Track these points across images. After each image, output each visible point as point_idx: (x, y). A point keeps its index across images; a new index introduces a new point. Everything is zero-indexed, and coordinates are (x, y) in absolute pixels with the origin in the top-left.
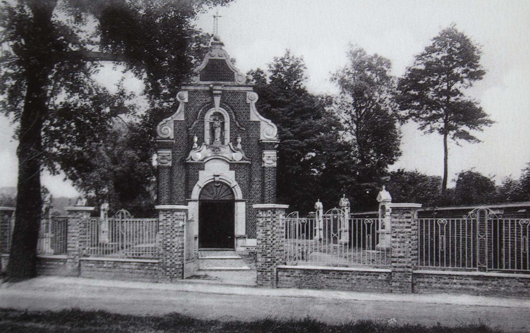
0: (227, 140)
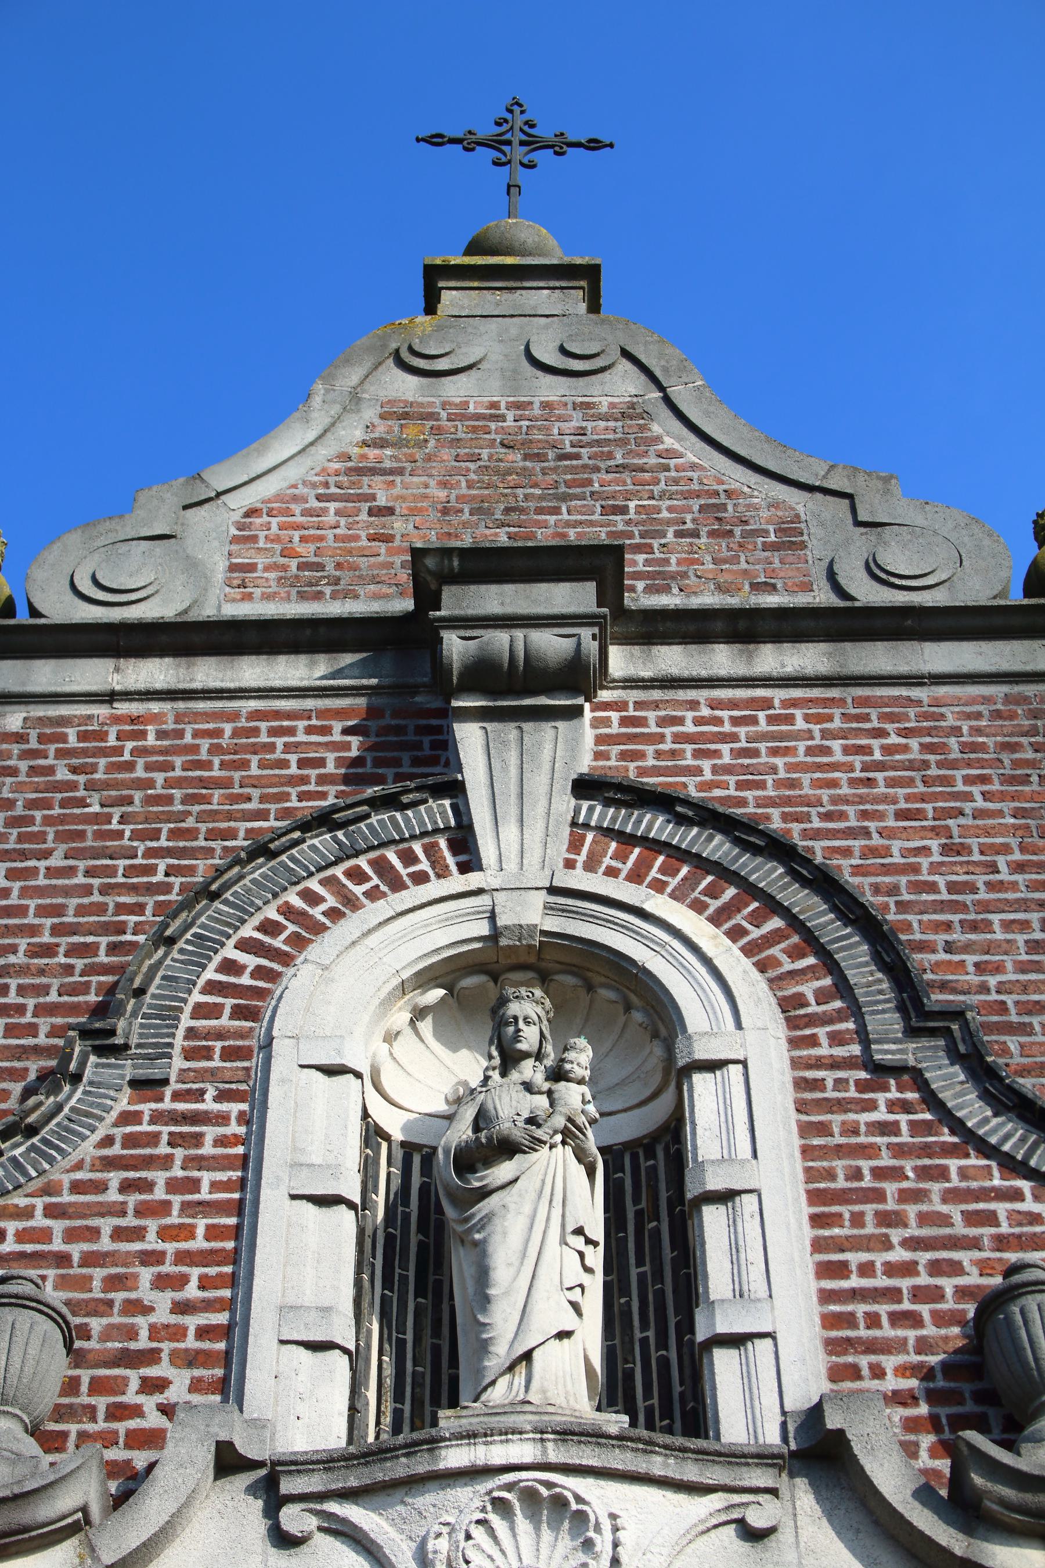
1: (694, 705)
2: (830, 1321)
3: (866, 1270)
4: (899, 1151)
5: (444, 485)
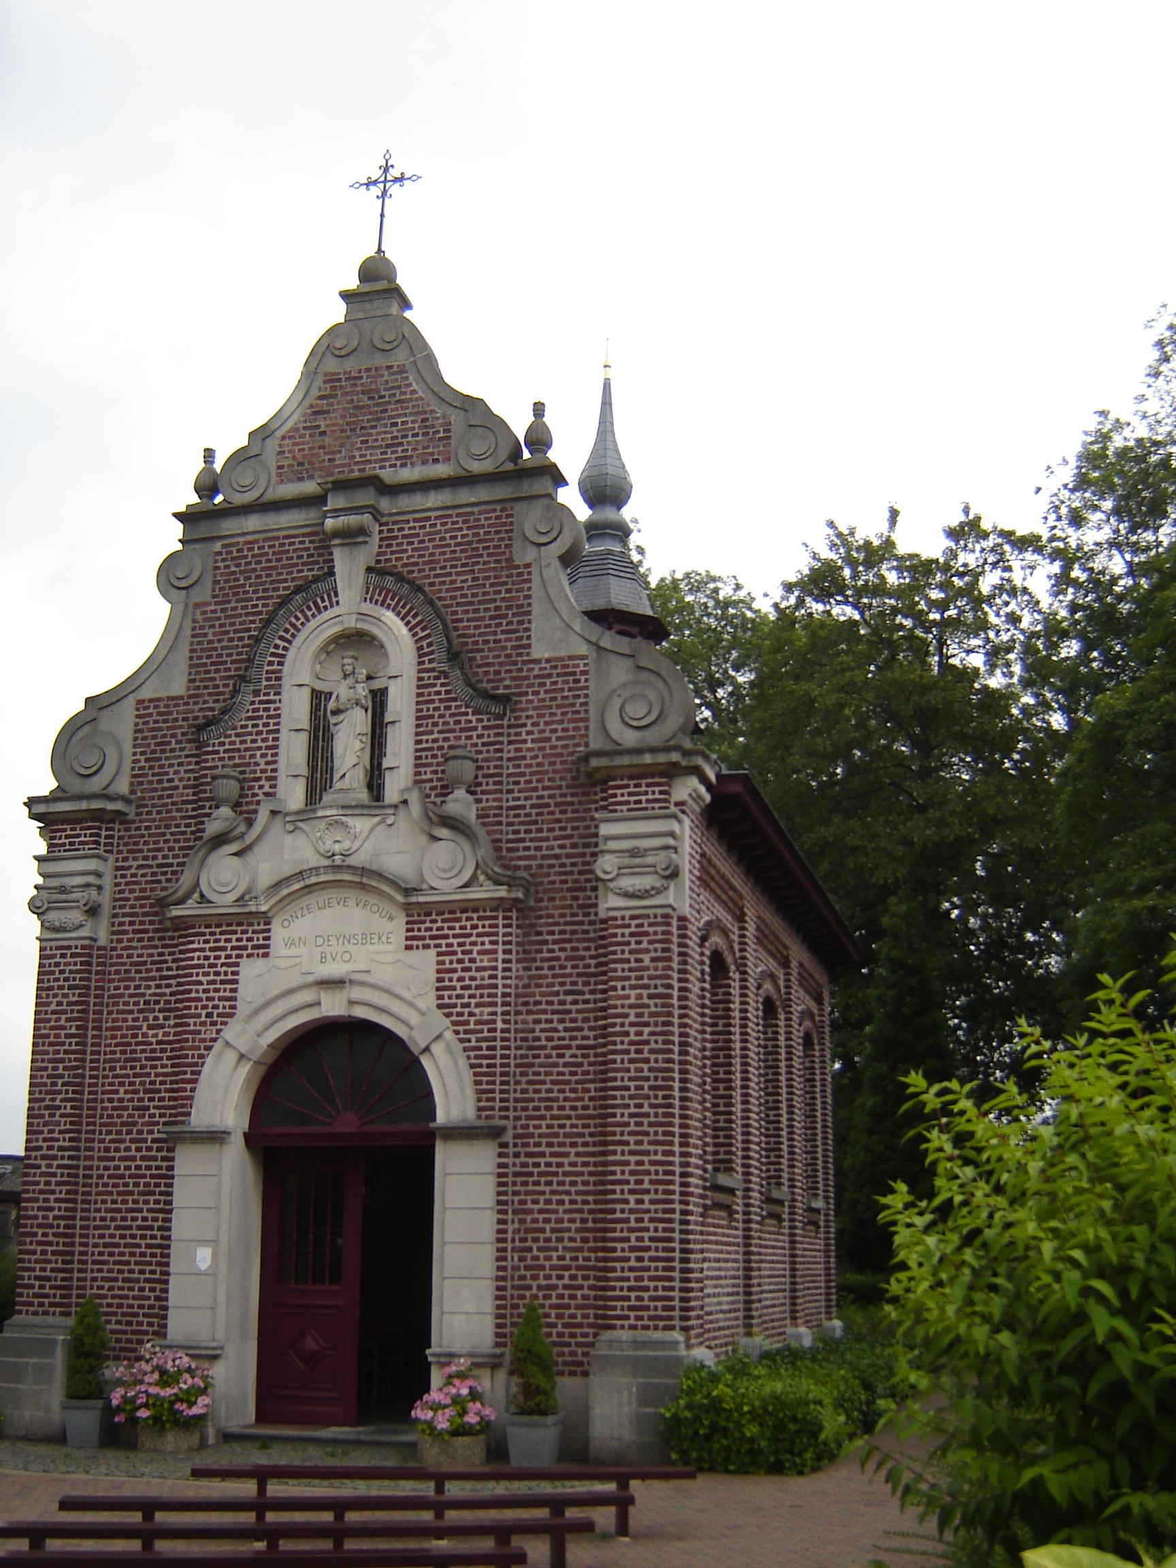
0: (396, 785)
1: (408, 522)
5: (343, 417)
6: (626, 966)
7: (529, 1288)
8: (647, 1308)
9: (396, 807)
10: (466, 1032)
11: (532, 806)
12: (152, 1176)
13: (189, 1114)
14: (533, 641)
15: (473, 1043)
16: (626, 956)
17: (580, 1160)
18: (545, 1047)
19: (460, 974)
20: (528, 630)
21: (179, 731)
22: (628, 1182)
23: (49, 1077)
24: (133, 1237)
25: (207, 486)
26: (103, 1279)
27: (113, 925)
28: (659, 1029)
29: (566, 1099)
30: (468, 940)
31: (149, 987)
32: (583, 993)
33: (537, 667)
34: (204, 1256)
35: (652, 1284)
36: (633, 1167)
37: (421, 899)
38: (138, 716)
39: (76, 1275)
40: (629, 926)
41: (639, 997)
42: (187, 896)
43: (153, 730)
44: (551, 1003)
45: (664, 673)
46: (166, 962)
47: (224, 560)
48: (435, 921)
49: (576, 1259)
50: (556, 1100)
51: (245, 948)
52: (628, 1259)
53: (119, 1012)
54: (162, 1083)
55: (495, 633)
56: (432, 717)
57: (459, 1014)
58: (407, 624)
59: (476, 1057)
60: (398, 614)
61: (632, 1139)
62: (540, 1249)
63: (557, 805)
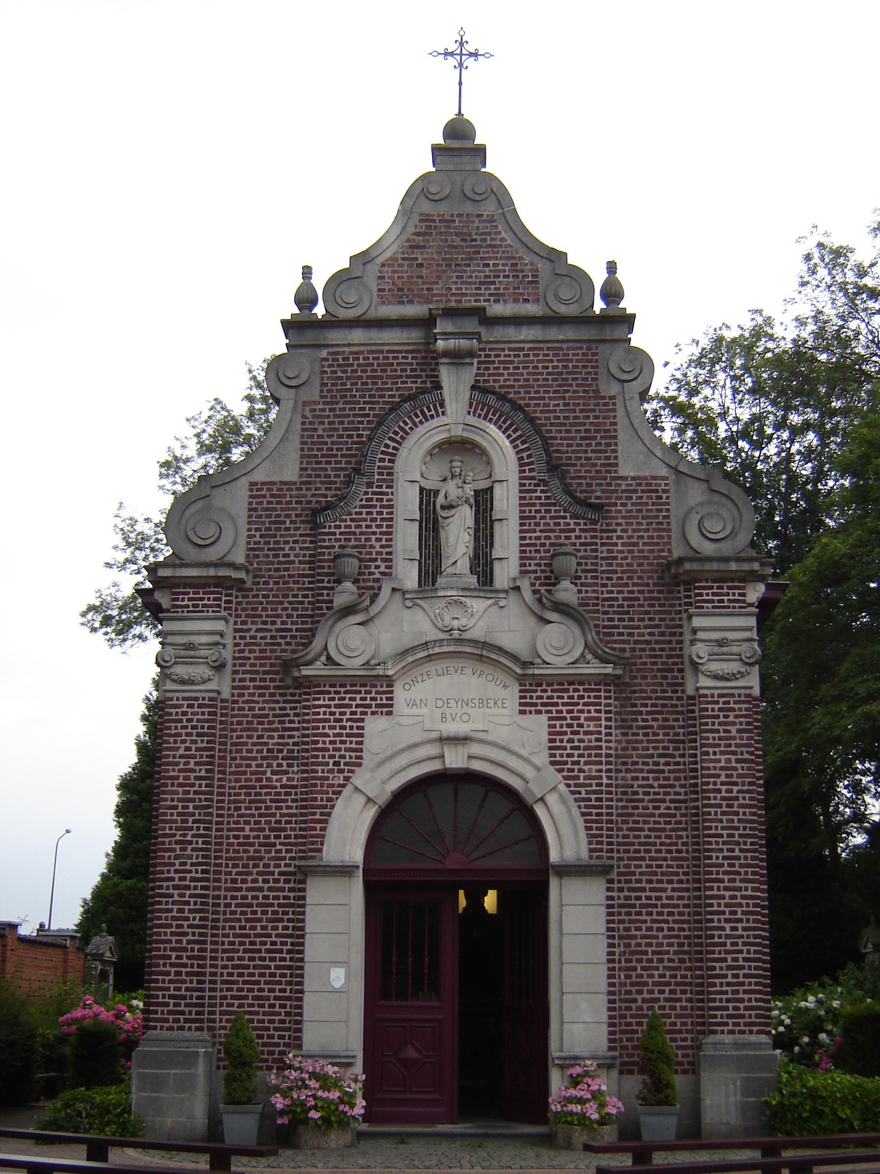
1: (503, 350)
2: (522, 552)
3: (530, 538)
4: (541, 505)
6: (717, 735)
7: (635, 1001)
8: (743, 1016)
9: (506, 592)
10: (576, 785)
11: (624, 599)
12: (279, 905)
13: (320, 850)
14: (620, 461)
15: (583, 795)
16: (716, 727)
17: (676, 894)
18: (642, 801)
19: (569, 736)
20: (615, 451)
21: (293, 513)
22: (724, 913)
23: (179, 814)
24: (262, 959)
25: (305, 299)
26: (232, 997)
27: (234, 680)
28: (746, 788)
29: (662, 844)
30: (576, 708)
31: (272, 737)
32: (674, 756)
33: (624, 483)
34: (338, 977)
35: (746, 997)
36: (727, 900)
37: (537, 672)
38: (251, 497)
39: (207, 994)
40: (717, 703)
41: (728, 761)
42: (316, 658)
43: (267, 509)
44: (647, 764)
45: (734, 497)
46: (288, 715)
47: (330, 366)
48: (545, 691)
49: (675, 976)
50: (655, 844)
51: (370, 706)
52: (726, 976)
53: (242, 758)
54: (287, 822)
55: (586, 452)
56: (535, 517)
57: (570, 770)
58: (508, 437)
59: (586, 807)
60: (500, 428)
61: (726, 877)
62: (643, 969)
63: (646, 599)
